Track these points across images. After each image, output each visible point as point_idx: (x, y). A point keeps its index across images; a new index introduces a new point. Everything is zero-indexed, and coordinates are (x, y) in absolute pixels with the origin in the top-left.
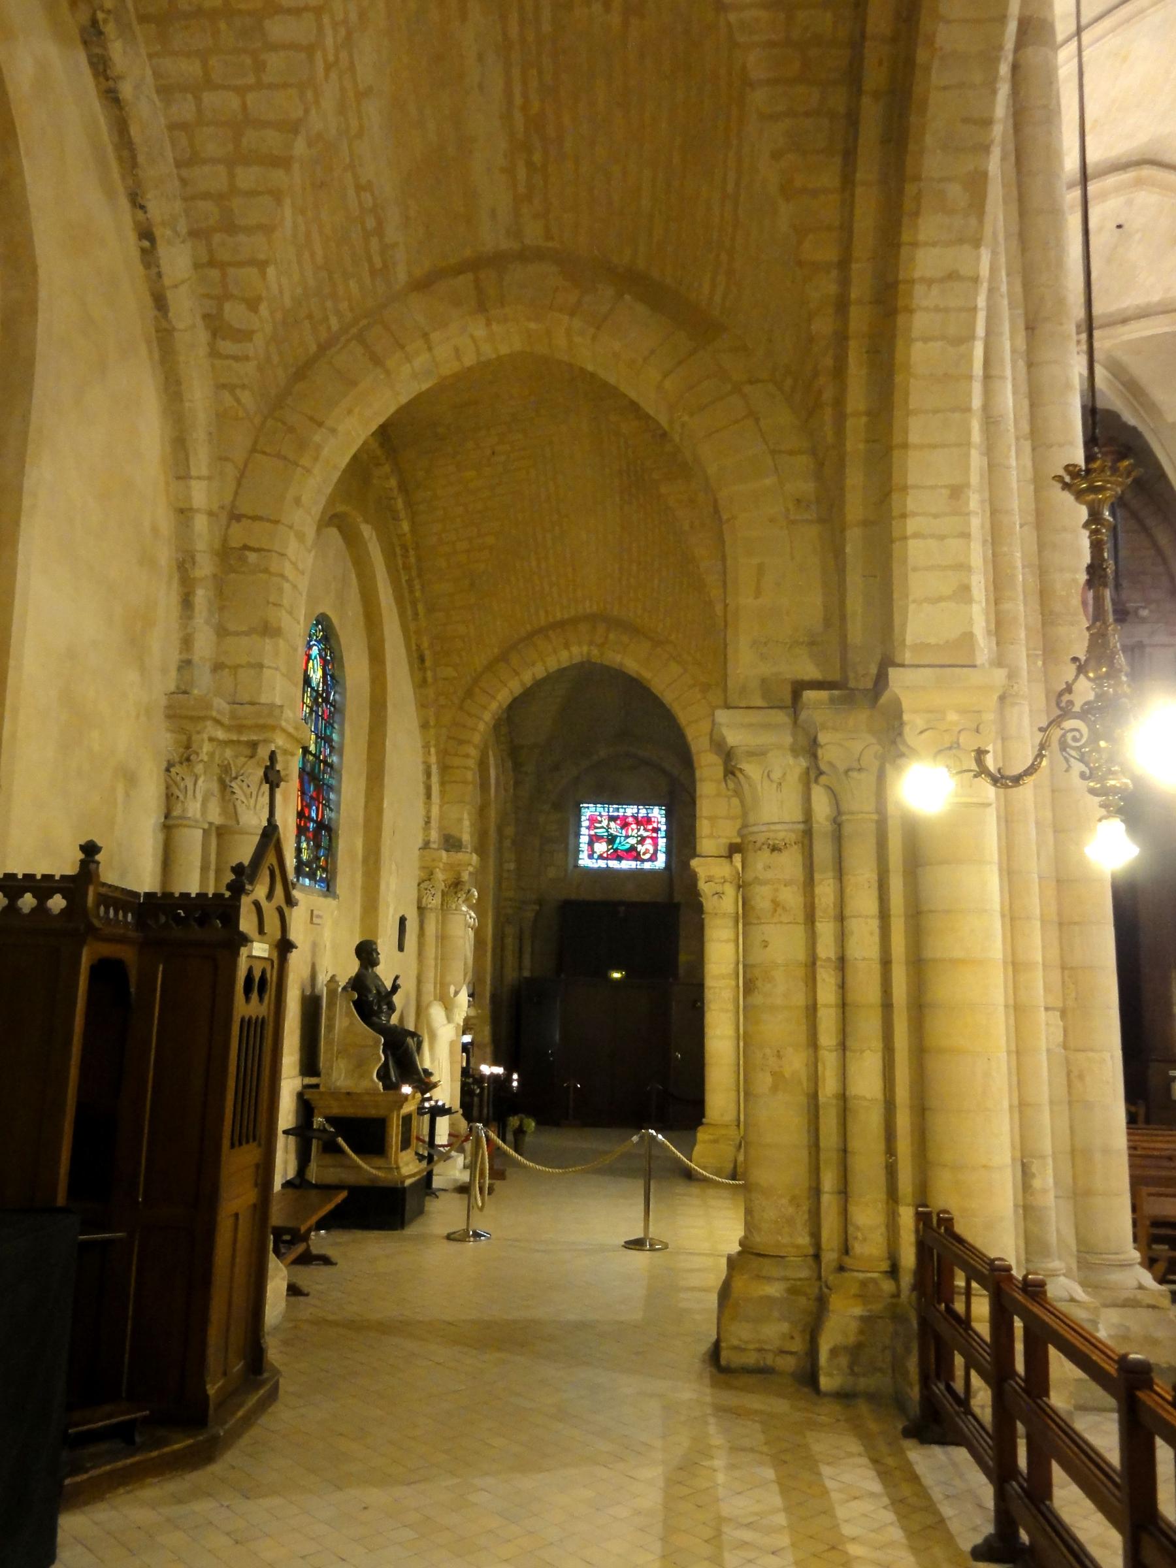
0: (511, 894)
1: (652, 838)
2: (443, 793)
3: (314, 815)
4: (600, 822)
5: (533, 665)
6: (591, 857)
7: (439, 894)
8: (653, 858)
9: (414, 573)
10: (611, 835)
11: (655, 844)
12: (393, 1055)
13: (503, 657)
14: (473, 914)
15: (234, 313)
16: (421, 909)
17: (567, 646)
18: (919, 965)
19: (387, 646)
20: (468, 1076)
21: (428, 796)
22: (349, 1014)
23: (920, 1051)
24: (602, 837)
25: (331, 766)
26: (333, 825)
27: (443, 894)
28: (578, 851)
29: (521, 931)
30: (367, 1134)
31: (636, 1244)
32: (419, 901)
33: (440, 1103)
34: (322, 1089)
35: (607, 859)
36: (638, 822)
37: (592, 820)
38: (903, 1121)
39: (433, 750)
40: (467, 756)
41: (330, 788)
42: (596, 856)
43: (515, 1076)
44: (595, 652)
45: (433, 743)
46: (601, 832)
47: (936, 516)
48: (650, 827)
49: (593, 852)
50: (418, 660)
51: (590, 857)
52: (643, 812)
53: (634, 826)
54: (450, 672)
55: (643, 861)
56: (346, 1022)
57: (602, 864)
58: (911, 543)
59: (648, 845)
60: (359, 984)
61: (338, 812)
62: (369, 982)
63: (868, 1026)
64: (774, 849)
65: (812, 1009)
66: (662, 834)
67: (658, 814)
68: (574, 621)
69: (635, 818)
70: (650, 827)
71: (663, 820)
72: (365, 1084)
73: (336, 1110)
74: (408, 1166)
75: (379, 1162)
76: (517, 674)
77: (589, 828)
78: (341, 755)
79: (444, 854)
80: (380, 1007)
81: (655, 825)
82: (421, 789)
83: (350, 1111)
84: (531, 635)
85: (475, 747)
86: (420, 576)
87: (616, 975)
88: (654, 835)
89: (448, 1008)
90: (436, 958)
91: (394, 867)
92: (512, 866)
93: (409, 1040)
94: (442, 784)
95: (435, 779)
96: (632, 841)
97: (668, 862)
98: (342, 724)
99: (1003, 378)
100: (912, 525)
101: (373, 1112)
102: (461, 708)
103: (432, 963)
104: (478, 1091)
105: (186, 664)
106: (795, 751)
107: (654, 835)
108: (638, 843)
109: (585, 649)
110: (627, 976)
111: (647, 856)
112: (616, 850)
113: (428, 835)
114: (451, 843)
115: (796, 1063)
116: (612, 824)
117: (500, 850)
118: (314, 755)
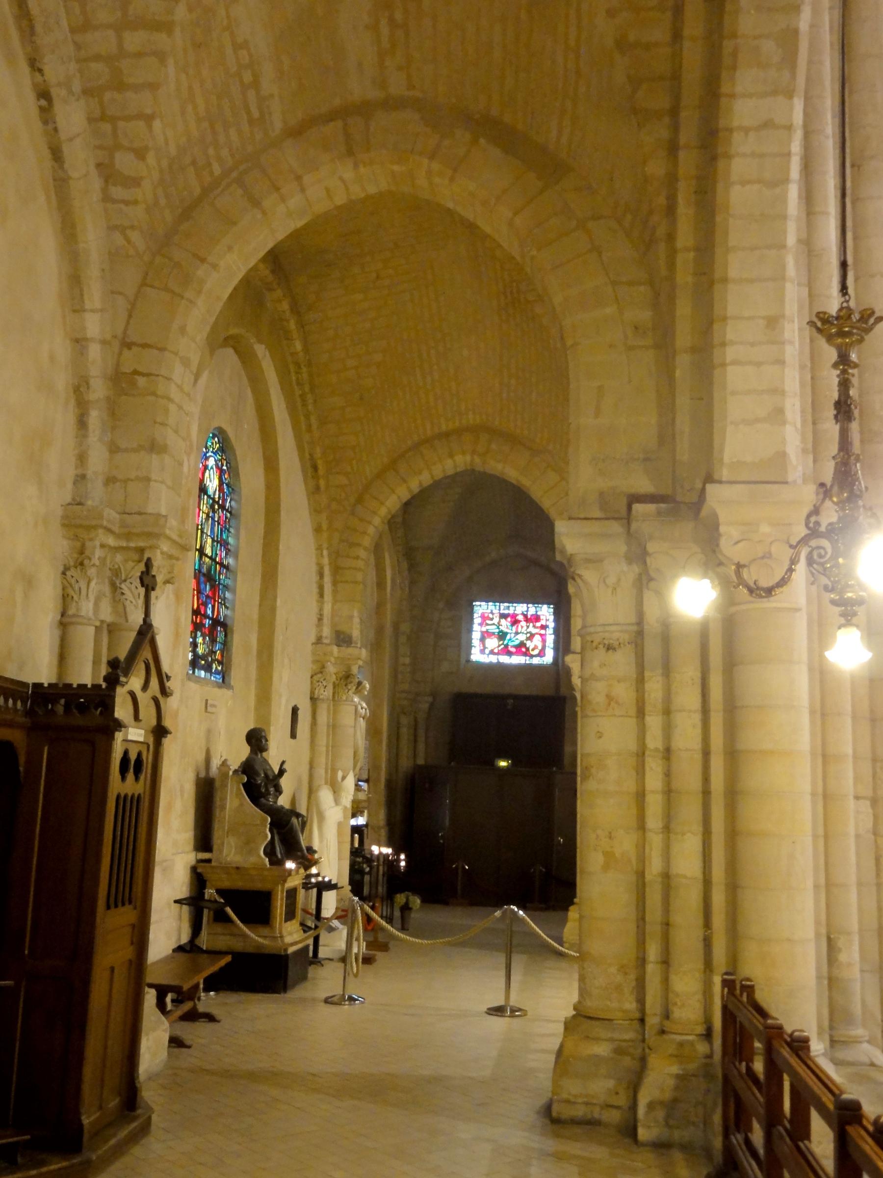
0: (406, 687)
1: (541, 635)
2: (335, 592)
3: (209, 612)
4: (492, 619)
5: (420, 473)
6: (482, 652)
7: (330, 688)
8: (541, 654)
9: (307, 388)
10: (502, 631)
11: (544, 641)
12: (279, 833)
13: (392, 465)
14: (364, 705)
15: (125, 162)
16: (313, 699)
17: (451, 456)
18: (733, 756)
19: (281, 454)
20: (359, 857)
21: (321, 595)
22: (238, 794)
23: (733, 835)
24: (493, 634)
25: (227, 567)
26: (229, 622)
27: (335, 686)
28: (470, 646)
29: (416, 720)
30: (254, 906)
31: (498, 1011)
32: (312, 693)
33: (327, 879)
34: (213, 864)
35: (498, 654)
36: (527, 620)
37: (484, 618)
38: (718, 898)
39: (325, 552)
40: (357, 558)
41: (226, 587)
42: (487, 651)
43: (403, 857)
44: (477, 460)
45: (325, 545)
46: (493, 629)
47: (752, 345)
49: (485, 648)
50: (311, 469)
51: (483, 652)
53: (523, 623)
54: (343, 480)
55: (532, 656)
56: (236, 803)
57: (493, 659)
58: (729, 369)
59: (537, 640)
60: (248, 768)
61: (233, 610)
62: (257, 767)
63: (690, 811)
64: (609, 648)
65: (640, 796)
66: (550, 631)
67: (546, 613)
68: (459, 432)
69: (525, 616)
70: (538, 624)
71: (552, 618)
72: (253, 859)
73: (226, 884)
74: (290, 936)
75: (265, 931)
76: (405, 481)
77: (481, 624)
78: (236, 557)
79: (335, 649)
80: (267, 790)
81: (543, 622)
82: (315, 590)
83: (240, 884)
84: (416, 446)
85: (365, 549)
86: (312, 390)
87: (503, 764)
88: (543, 632)
89: (336, 789)
90: (327, 746)
91: (286, 661)
92: (407, 660)
93: (294, 820)
94: (335, 583)
95: (327, 579)
96: (522, 637)
97: (556, 659)
98: (238, 530)
99: (827, 214)
100: (731, 353)
101: (258, 886)
102: (353, 513)
103: (324, 749)
104: (368, 869)
105: (81, 478)
106: (629, 559)
107: (543, 632)
108: (528, 639)
109: (468, 458)
110: (513, 764)
111: (536, 652)
113: (321, 631)
114: (342, 639)
115: (626, 844)
116: (503, 621)
117: (396, 647)
118: (211, 558)
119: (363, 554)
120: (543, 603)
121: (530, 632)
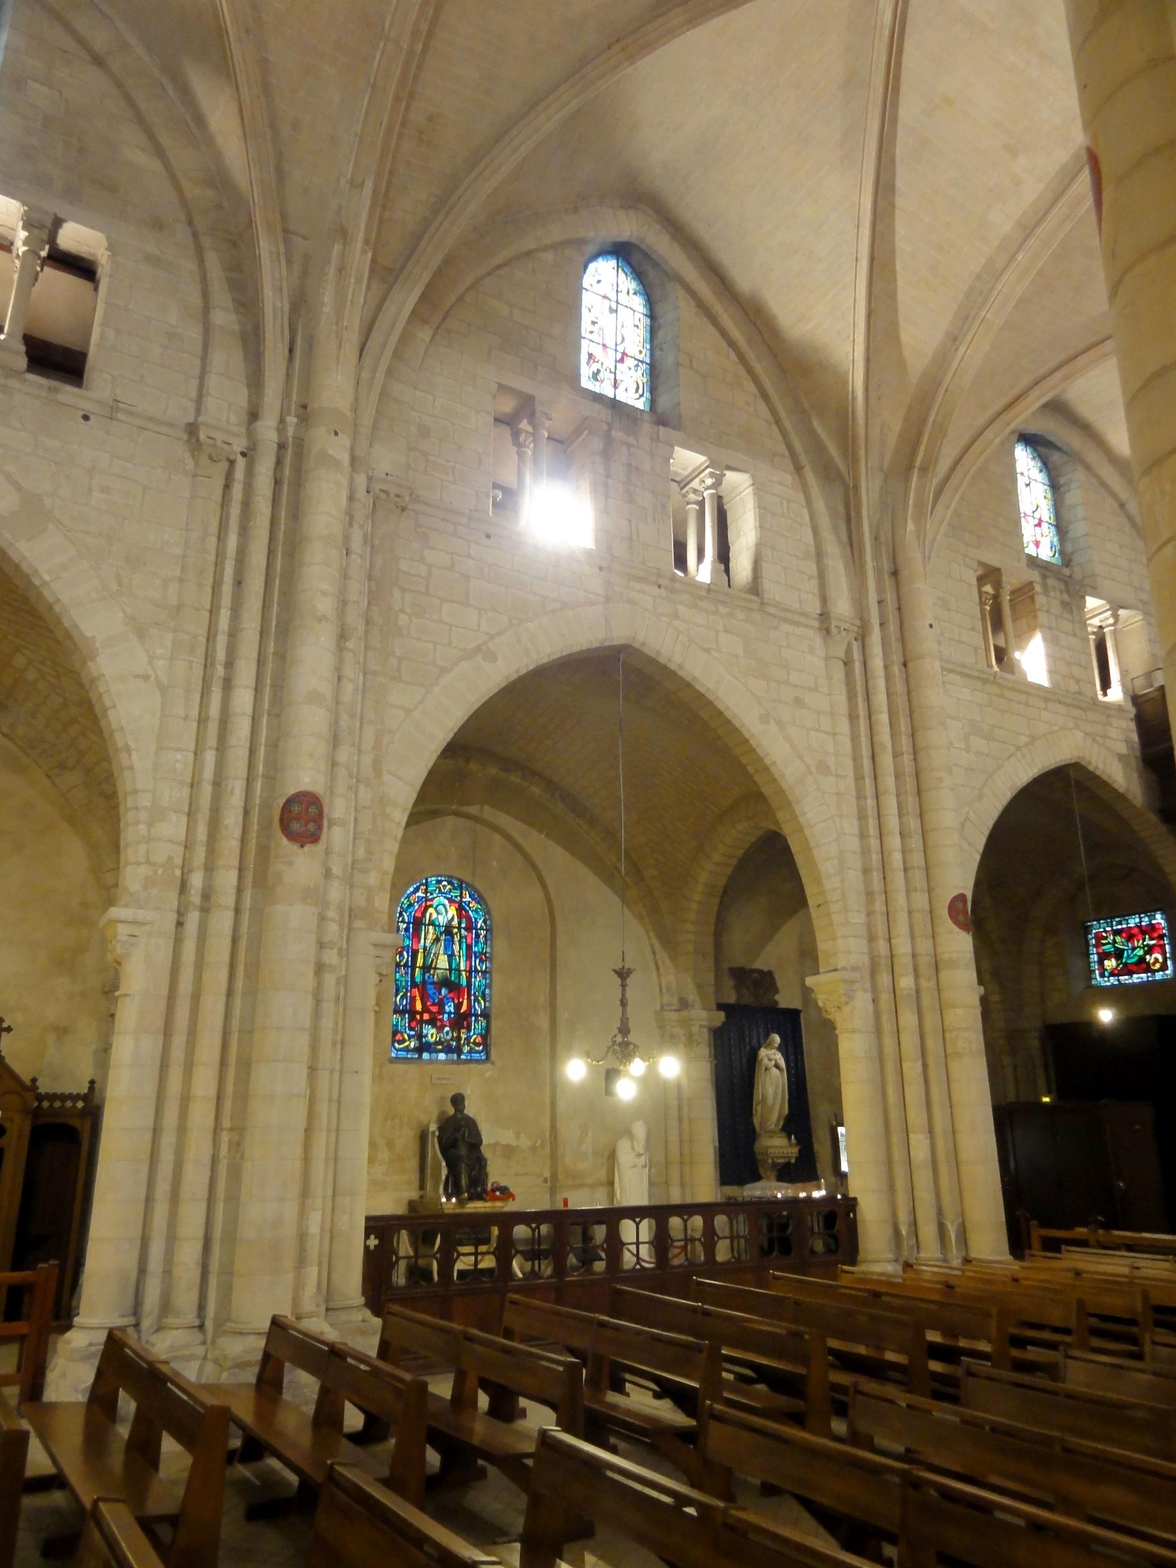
4: (1106, 938)
6: (1102, 975)
8: (1164, 967)
11: (1164, 953)
35: (1118, 975)
37: (1099, 937)
48: (1156, 935)
52: (1145, 921)
53: (1140, 937)
67: (1159, 919)
70: (1156, 935)
108: (1146, 953)
111: (1158, 966)
112: (1126, 965)
116: (1118, 939)
119: (690, 927)
120: (1156, 911)
121: (1148, 945)
